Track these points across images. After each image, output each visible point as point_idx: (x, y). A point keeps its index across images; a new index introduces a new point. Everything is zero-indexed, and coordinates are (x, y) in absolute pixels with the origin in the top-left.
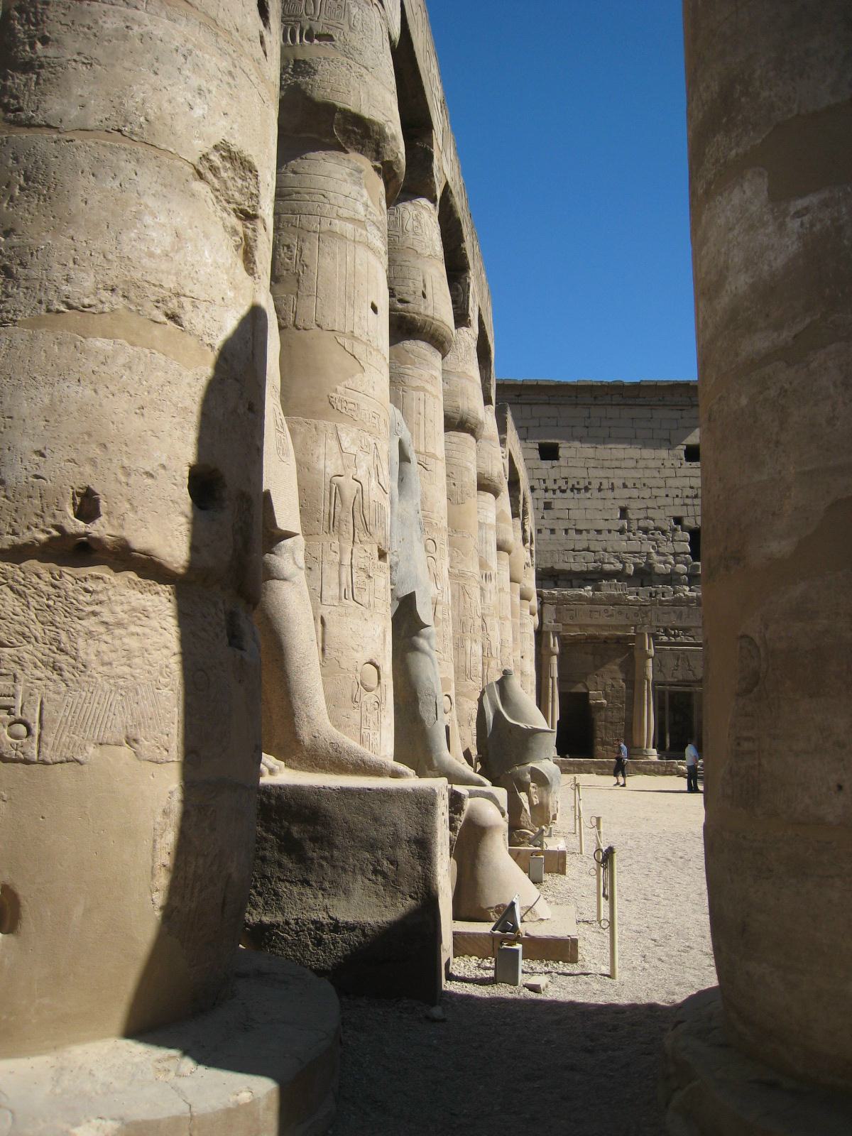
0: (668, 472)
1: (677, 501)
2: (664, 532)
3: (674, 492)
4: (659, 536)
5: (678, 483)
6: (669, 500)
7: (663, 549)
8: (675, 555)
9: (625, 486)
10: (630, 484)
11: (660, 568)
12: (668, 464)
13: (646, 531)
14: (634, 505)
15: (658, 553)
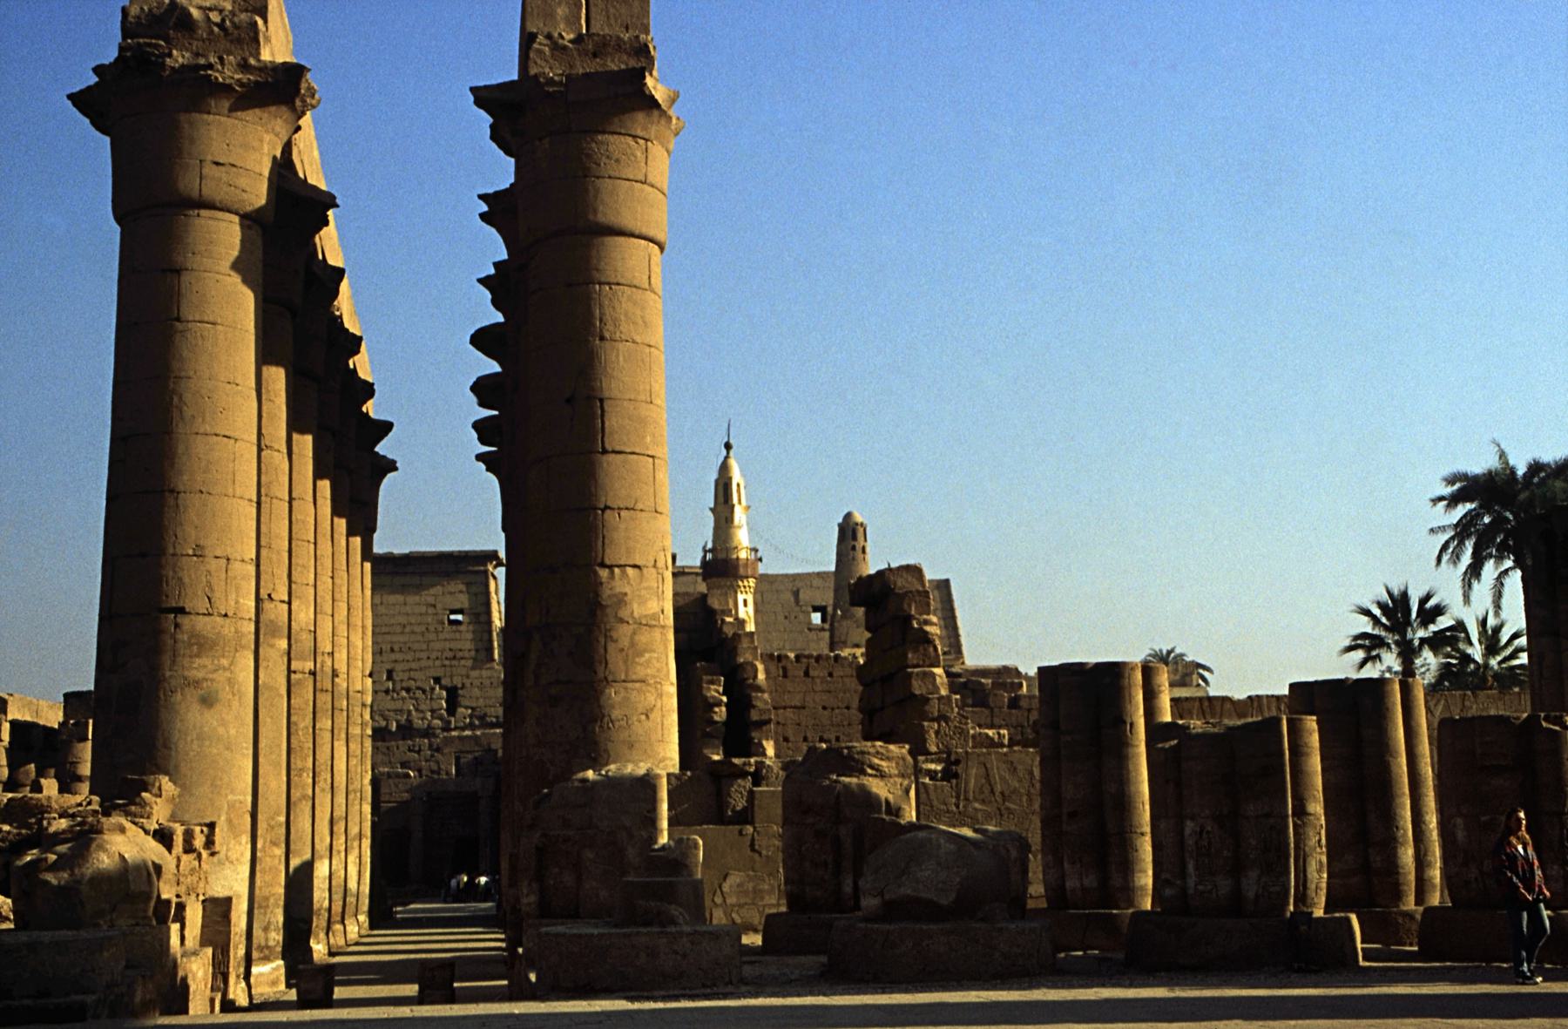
0: (432, 636)
1: (438, 663)
2: (424, 691)
3: (434, 656)
4: (419, 694)
5: (438, 646)
6: (430, 663)
7: (423, 707)
8: (433, 711)
9: (392, 650)
10: (396, 648)
11: (418, 723)
12: (432, 628)
13: (408, 690)
14: (399, 667)
15: (417, 710)
